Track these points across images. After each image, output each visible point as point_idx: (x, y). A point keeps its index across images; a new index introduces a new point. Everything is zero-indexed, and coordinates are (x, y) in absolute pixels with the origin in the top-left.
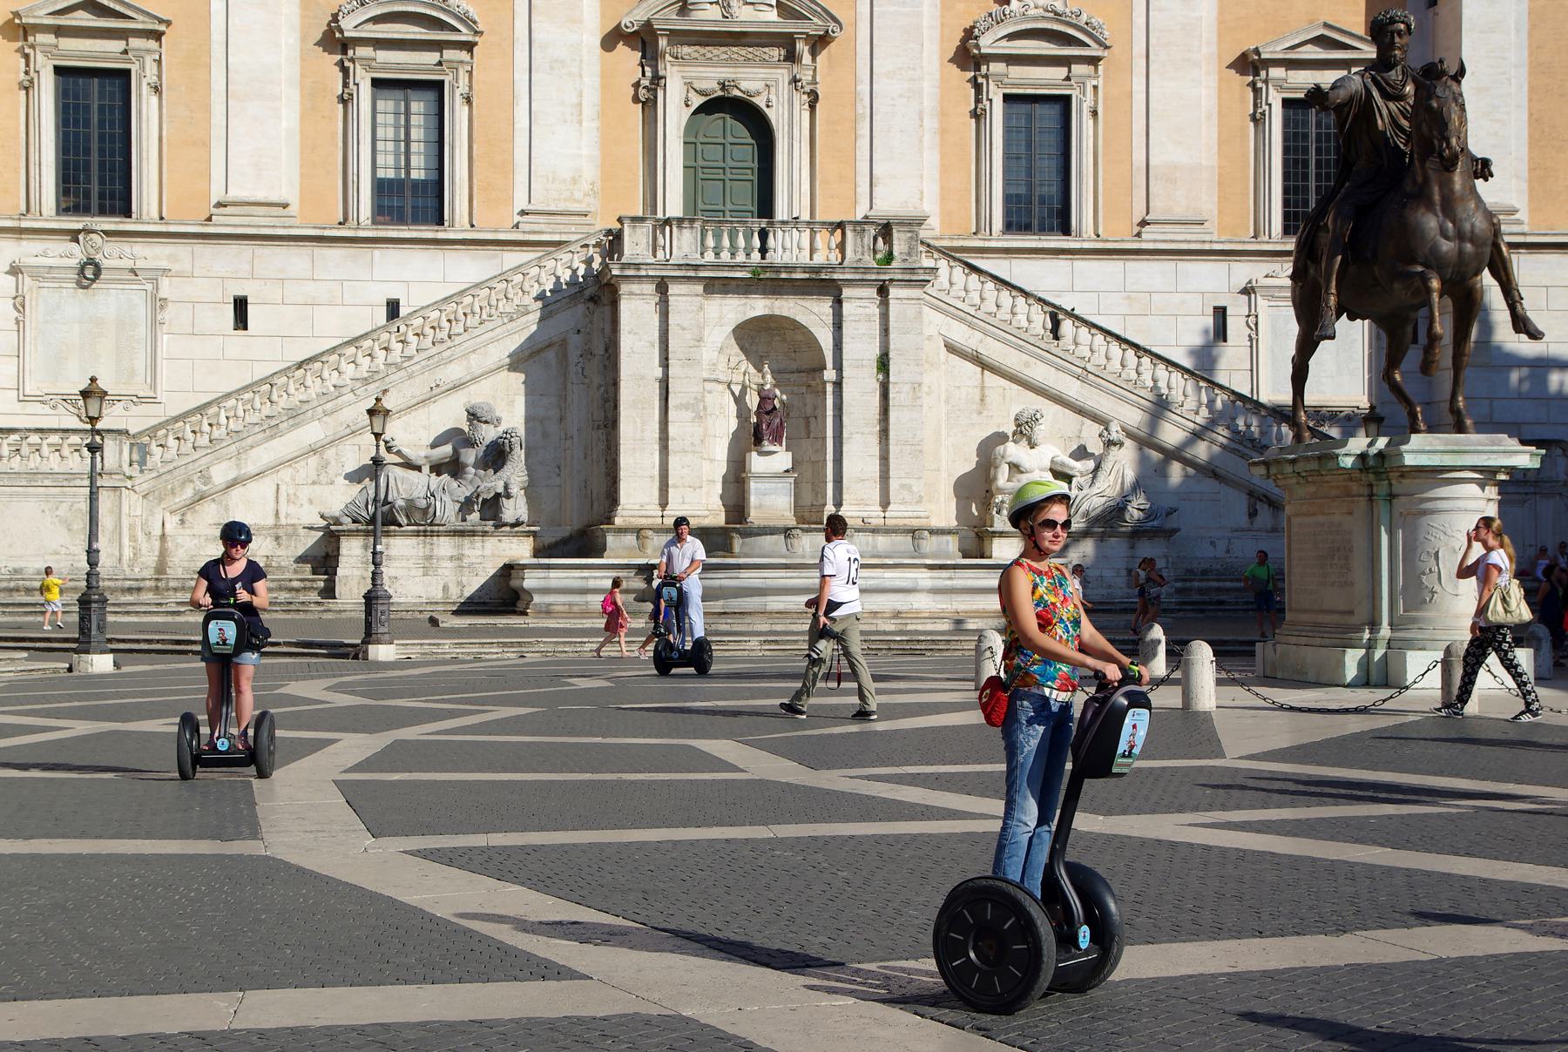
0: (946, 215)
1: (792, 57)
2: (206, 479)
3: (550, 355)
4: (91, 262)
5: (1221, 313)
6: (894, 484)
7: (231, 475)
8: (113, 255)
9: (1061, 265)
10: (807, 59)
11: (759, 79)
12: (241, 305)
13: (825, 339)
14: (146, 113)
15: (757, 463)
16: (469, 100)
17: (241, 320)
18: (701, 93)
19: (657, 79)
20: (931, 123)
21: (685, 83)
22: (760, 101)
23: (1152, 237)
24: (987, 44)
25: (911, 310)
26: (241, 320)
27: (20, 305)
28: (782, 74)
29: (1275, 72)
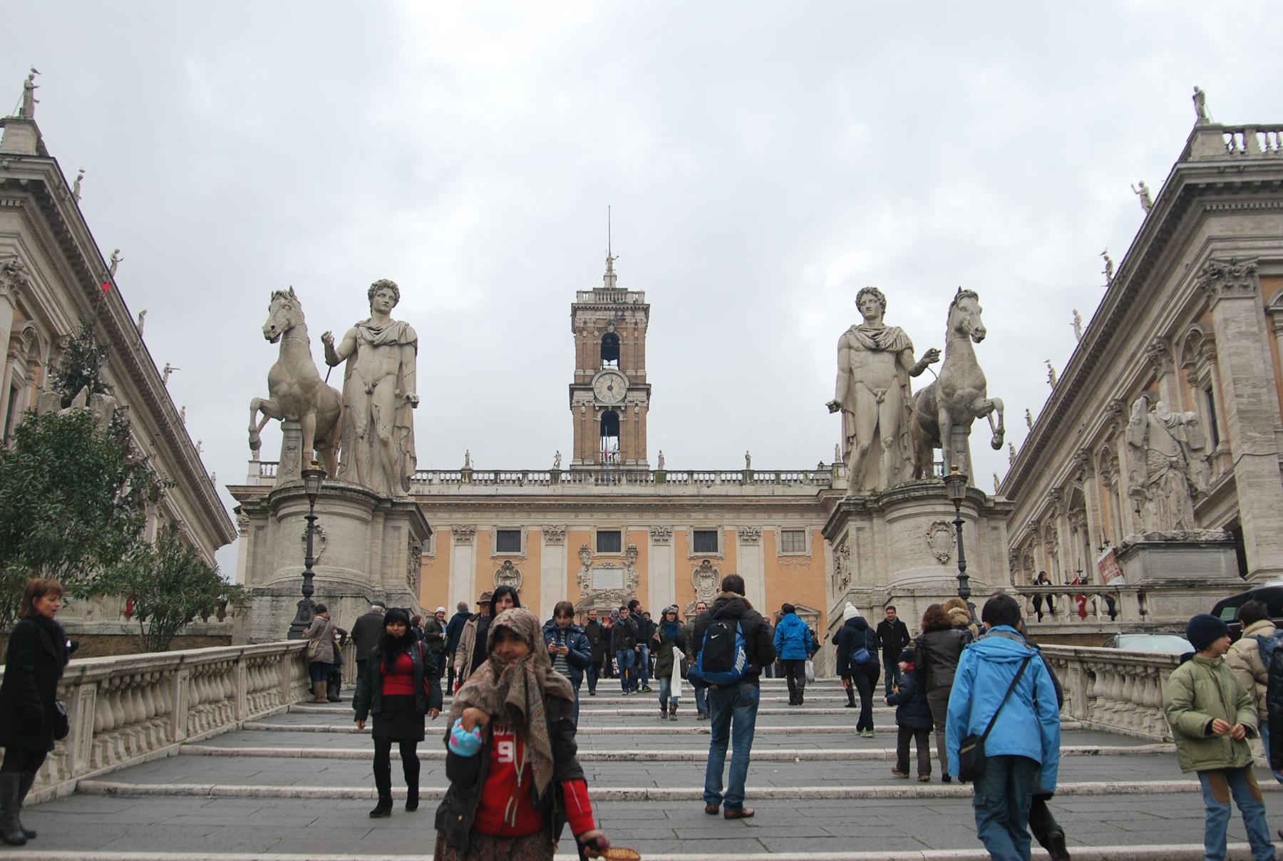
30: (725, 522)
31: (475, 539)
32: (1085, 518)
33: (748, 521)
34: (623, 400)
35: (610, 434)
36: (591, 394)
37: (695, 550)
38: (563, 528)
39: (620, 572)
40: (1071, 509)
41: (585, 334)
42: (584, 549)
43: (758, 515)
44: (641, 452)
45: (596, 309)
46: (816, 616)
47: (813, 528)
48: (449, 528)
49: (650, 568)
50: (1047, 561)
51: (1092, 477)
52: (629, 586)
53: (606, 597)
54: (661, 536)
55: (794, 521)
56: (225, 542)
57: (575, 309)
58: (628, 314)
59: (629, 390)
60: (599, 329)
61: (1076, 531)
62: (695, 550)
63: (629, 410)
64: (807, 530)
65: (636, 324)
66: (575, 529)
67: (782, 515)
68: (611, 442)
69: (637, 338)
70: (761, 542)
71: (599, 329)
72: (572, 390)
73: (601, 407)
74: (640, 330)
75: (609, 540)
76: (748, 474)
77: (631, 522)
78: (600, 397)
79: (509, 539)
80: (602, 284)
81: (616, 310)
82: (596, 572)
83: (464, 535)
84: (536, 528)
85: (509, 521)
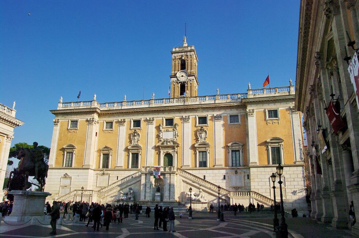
0: (192, 165)
1: (174, 149)
2: (104, 195)
3: (139, 182)
4: (104, 173)
6: (171, 197)
7: (107, 195)
8: (106, 172)
9: (205, 171)
10: (176, 148)
11: (170, 151)
12: (118, 177)
15: (157, 194)
17: (117, 179)
18: (165, 153)
19: (160, 152)
21: (163, 152)
22: (171, 153)
25: (173, 176)
26: (117, 179)
27: (97, 177)
29: (230, 147)
31: (125, 124)
32: (337, 64)
33: (216, 113)
37: (199, 124)
40: (328, 60)
42: (160, 125)
46: (242, 146)
47: (241, 114)
52: (175, 137)
55: (234, 112)
59: (188, 76)
61: (332, 74)
62: (199, 124)
63: (188, 82)
64: (239, 115)
65: (191, 56)
67: (230, 110)
71: (179, 59)
73: (179, 82)
79: (137, 123)
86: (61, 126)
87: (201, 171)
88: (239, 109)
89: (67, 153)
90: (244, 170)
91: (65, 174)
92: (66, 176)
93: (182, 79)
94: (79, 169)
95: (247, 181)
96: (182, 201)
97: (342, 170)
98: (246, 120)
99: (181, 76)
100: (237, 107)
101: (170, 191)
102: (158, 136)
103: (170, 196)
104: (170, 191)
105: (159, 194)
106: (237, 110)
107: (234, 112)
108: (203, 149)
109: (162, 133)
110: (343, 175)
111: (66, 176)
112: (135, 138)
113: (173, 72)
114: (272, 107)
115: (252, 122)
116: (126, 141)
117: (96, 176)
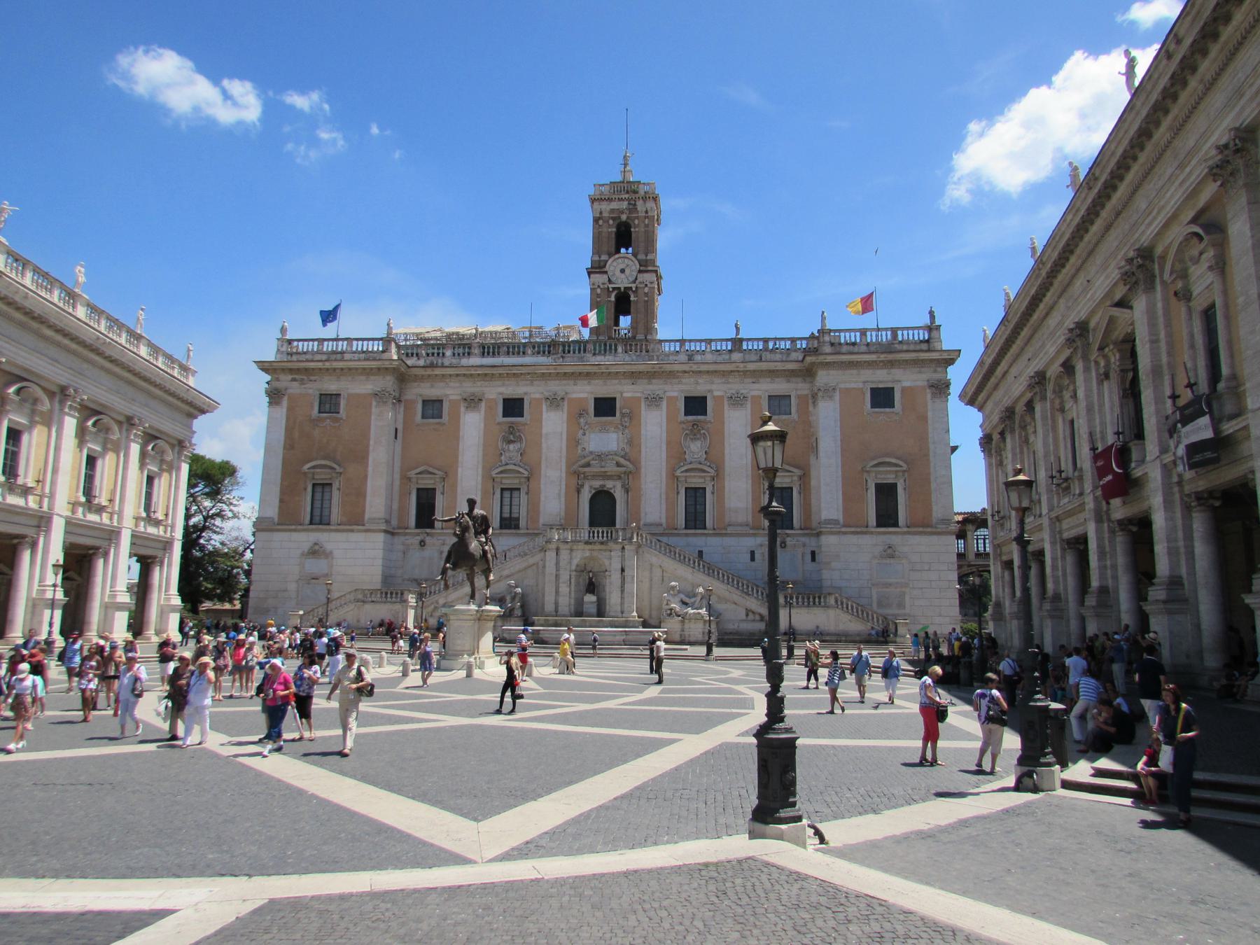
5: (753, 553)
13: (607, 562)
14: (440, 502)
16: (527, 493)
20: (664, 497)
23: (730, 530)
24: (678, 473)
28: (619, 484)
30: (714, 387)
33: (735, 386)
34: (634, 282)
35: (627, 313)
36: (605, 276)
38: (561, 394)
39: (614, 436)
41: (601, 222)
43: (747, 380)
44: (649, 329)
45: (610, 200)
48: (459, 397)
49: (643, 432)
50: (1054, 421)
51: (1150, 287)
53: (600, 457)
54: (654, 401)
55: (780, 387)
56: (203, 412)
57: (593, 201)
58: (640, 204)
59: (640, 271)
60: (614, 219)
66: (574, 396)
68: (625, 321)
69: (647, 226)
70: (749, 405)
71: (614, 219)
72: (589, 273)
73: (614, 289)
74: (652, 221)
75: (605, 407)
76: (737, 342)
77: (626, 388)
78: (613, 279)
80: (619, 179)
81: (628, 200)
82: (592, 436)
83: (472, 402)
84: (537, 396)
85: (513, 390)
86: (290, 410)
87: (691, 539)
88: (794, 379)
89: (314, 485)
90: (803, 539)
91: (310, 544)
92: (315, 552)
93: (622, 282)
94: (352, 531)
95: (810, 566)
96: (650, 616)
97: (1114, 567)
98: (811, 408)
99: (622, 269)
100: (791, 374)
101: (622, 591)
102: (573, 442)
103: (622, 604)
104: (622, 591)
105: (593, 598)
106: (788, 381)
107: (780, 387)
108: (696, 481)
109: (586, 438)
110: (1115, 578)
111: (315, 552)
112: (511, 447)
113: (596, 258)
114: (881, 377)
115: (827, 416)
116: (484, 455)
117: (401, 547)
